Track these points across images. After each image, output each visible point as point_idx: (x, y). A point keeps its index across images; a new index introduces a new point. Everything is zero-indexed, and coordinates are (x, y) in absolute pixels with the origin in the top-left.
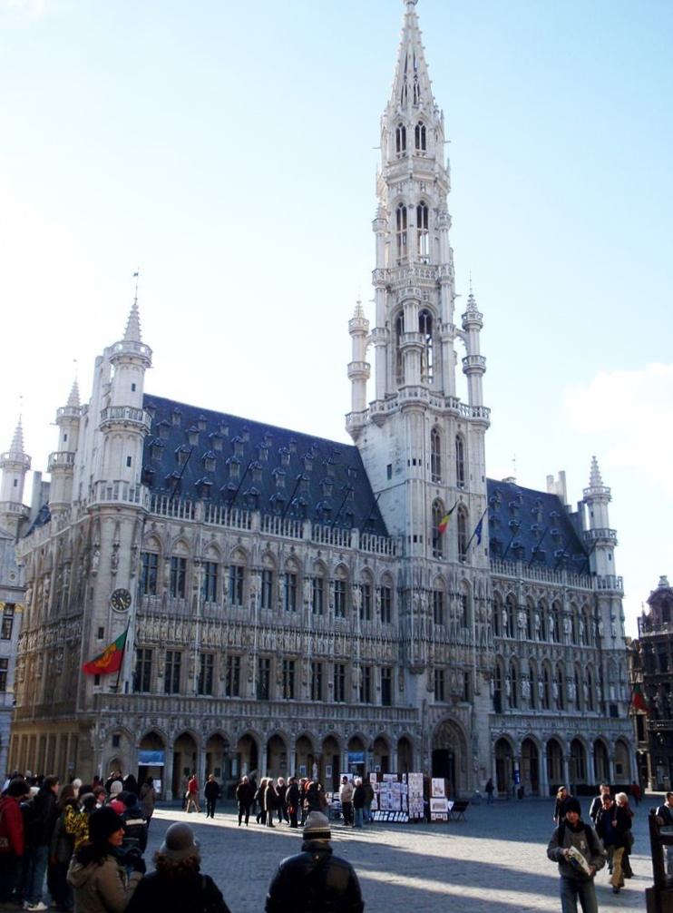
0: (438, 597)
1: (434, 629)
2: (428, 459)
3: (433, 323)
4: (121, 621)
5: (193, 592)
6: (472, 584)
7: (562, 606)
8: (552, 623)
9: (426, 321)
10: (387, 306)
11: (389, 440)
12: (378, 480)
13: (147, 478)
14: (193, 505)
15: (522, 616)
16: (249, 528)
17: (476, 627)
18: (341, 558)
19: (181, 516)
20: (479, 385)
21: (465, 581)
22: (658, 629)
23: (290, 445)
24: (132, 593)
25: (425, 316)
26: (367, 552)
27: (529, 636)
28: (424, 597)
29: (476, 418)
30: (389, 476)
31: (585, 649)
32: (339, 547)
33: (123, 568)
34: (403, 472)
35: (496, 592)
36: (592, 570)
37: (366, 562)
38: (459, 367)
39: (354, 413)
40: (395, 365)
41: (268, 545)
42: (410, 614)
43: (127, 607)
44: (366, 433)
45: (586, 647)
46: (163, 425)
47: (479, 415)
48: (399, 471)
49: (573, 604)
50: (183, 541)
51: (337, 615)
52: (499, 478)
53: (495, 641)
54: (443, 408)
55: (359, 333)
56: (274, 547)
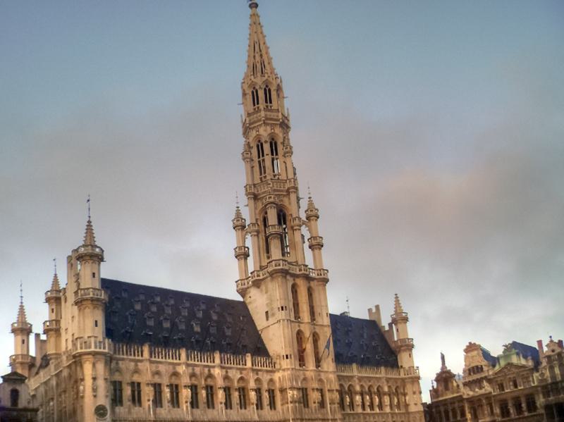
0: (304, 391)
1: (303, 411)
2: (291, 306)
3: (287, 218)
7: (382, 388)
8: (377, 400)
9: (282, 217)
10: (256, 208)
11: (265, 296)
12: (260, 322)
13: (109, 333)
14: (142, 348)
15: (358, 398)
16: (180, 359)
17: (331, 408)
18: (241, 373)
19: (134, 355)
20: (320, 254)
21: (320, 380)
22: (442, 396)
23: (201, 304)
24: (108, 407)
25: (282, 214)
26: (257, 368)
27: (364, 408)
28: (295, 392)
30: (267, 319)
31: (399, 413)
32: (239, 366)
33: (102, 391)
34: (276, 316)
35: (341, 385)
36: (400, 365)
37: (257, 374)
38: (307, 244)
39: (241, 280)
40: (265, 247)
41: (193, 369)
42: (288, 403)
44: (250, 292)
45: (399, 412)
46: (116, 298)
47: (321, 275)
48: (273, 315)
49: (389, 387)
50: (136, 371)
51: (241, 408)
52: (338, 313)
53: (343, 415)
54: (298, 273)
55: (240, 227)
56: (197, 370)
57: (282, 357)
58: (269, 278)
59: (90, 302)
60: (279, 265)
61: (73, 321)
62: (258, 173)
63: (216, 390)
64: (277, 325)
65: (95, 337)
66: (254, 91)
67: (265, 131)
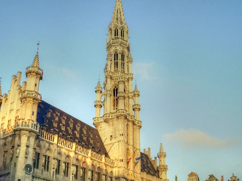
2: (126, 135)
4: (28, 177)
5: (52, 170)
6: (136, 177)
11: (111, 127)
16: (72, 149)
19: (49, 140)
29: (138, 124)
32: (99, 160)
33: (31, 156)
34: (117, 138)
36: (160, 177)
43: (30, 172)
44: (101, 125)
47: (139, 123)
48: (115, 138)
50: (49, 149)
57: (119, 160)
58: (115, 119)
59: (32, 99)
60: (124, 113)
61: (10, 113)
62: (114, 67)
63: (87, 171)
64: (118, 143)
65: (33, 121)
66: (116, 29)
67: (120, 48)
